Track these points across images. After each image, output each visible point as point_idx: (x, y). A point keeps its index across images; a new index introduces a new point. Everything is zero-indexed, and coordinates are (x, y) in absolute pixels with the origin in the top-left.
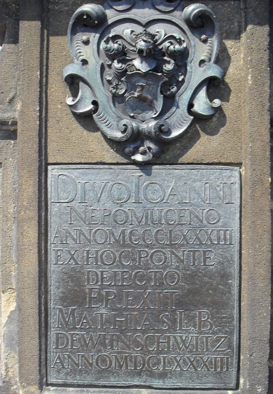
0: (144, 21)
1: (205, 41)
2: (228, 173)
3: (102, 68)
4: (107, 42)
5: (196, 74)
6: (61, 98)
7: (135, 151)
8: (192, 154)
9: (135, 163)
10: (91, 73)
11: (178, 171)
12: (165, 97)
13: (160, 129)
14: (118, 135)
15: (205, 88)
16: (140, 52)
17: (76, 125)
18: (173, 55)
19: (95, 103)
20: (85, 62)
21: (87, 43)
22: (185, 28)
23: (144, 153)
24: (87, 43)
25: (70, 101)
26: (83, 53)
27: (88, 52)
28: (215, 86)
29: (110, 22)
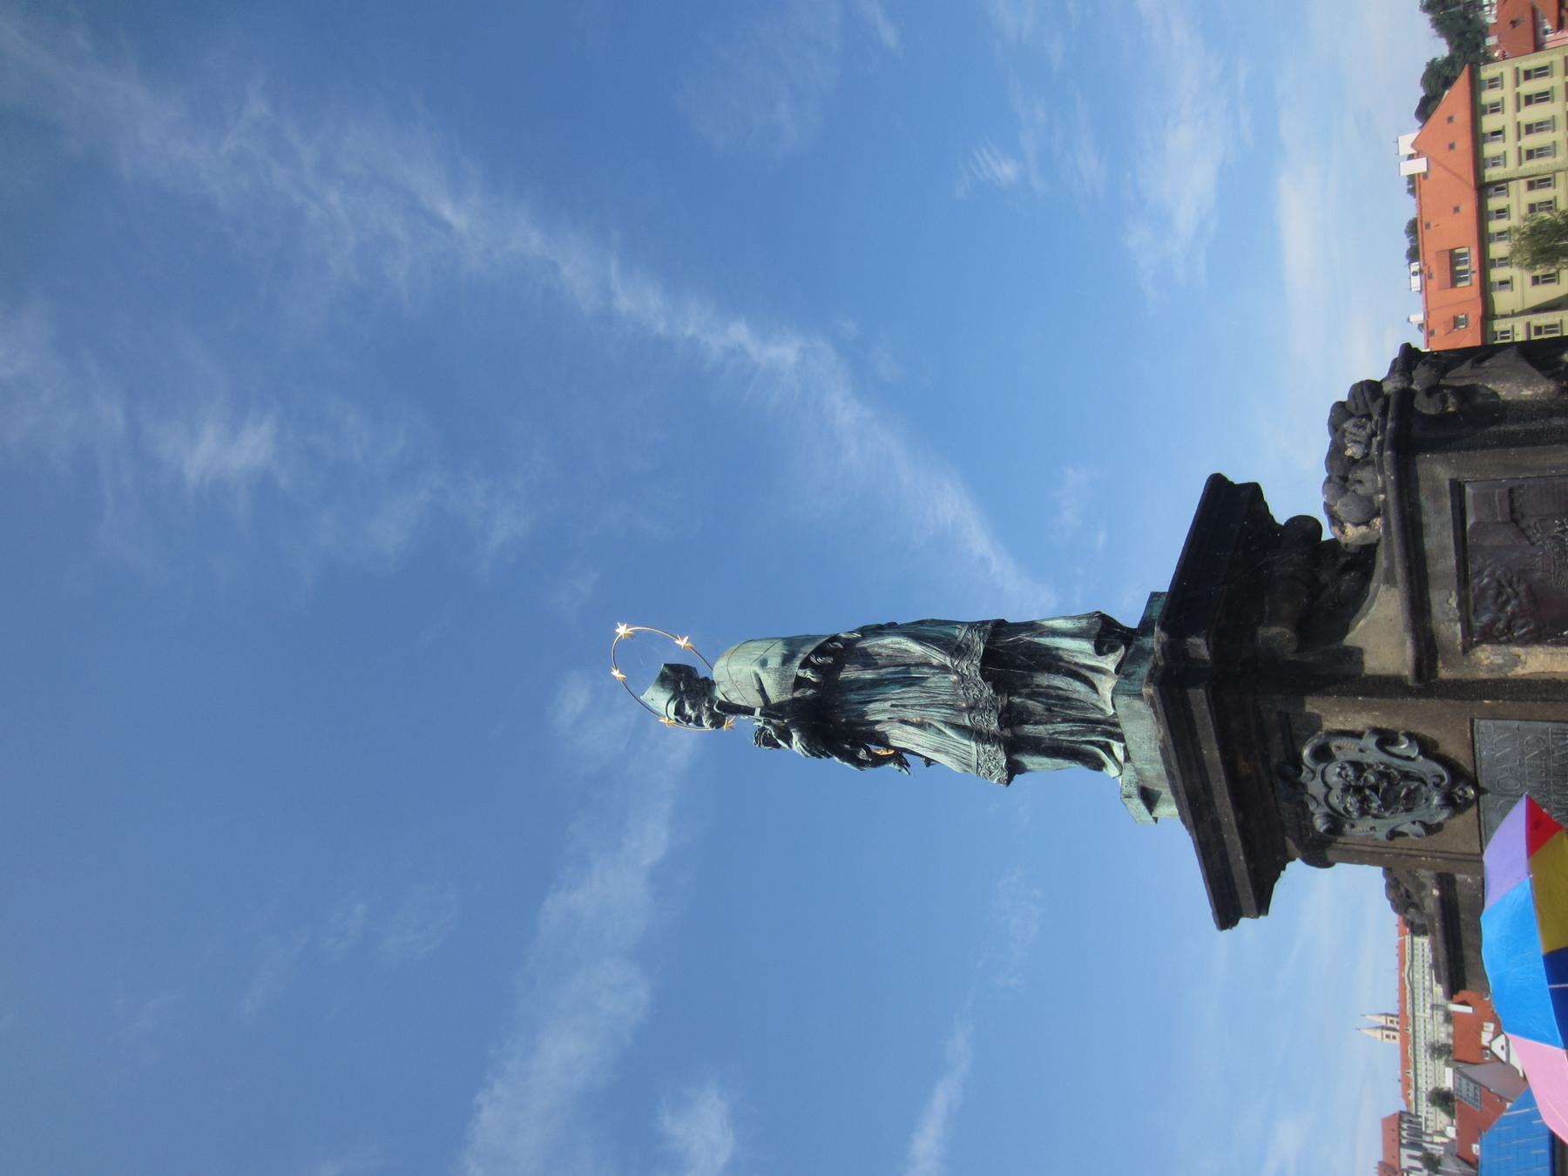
0: (1324, 790)
2: (1482, 729)
3: (1375, 817)
11: (1483, 766)
28: (1386, 739)
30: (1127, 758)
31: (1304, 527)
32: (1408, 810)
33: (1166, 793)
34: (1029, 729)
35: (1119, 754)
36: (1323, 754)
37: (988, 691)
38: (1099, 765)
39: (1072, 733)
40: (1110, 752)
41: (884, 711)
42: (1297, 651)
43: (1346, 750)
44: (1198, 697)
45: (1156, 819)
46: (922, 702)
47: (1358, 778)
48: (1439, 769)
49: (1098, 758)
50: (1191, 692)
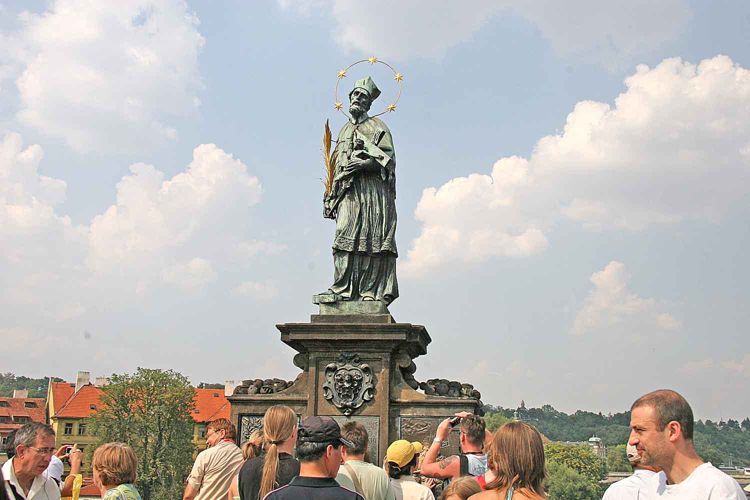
1: (368, 376)
3: (335, 384)
4: (337, 376)
5: (365, 387)
6: (322, 394)
7: (345, 412)
8: (364, 413)
9: (345, 415)
10: (332, 386)
12: (355, 394)
13: (352, 404)
14: (340, 406)
15: (367, 391)
16: (346, 380)
17: (327, 402)
18: (357, 381)
19: (333, 396)
20: (330, 382)
21: (330, 376)
22: (362, 371)
23: (348, 412)
24: (330, 376)
25: (325, 395)
26: (329, 380)
27: (330, 379)
28: (371, 391)
29: (338, 369)
30: (343, 298)
31: (413, 368)
32: (339, 394)
33: (333, 311)
34: (357, 262)
35: (345, 294)
36: (366, 370)
37: (376, 250)
38: (338, 284)
39: (354, 278)
40: (344, 291)
41: (366, 202)
42: (399, 366)
43: (367, 378)
44: (403, 337)
45: (318, 304)
46: (371, 220)
47: (355, 380)
48: (358, 406)
49: (343, 286)
50: (405, 335)
